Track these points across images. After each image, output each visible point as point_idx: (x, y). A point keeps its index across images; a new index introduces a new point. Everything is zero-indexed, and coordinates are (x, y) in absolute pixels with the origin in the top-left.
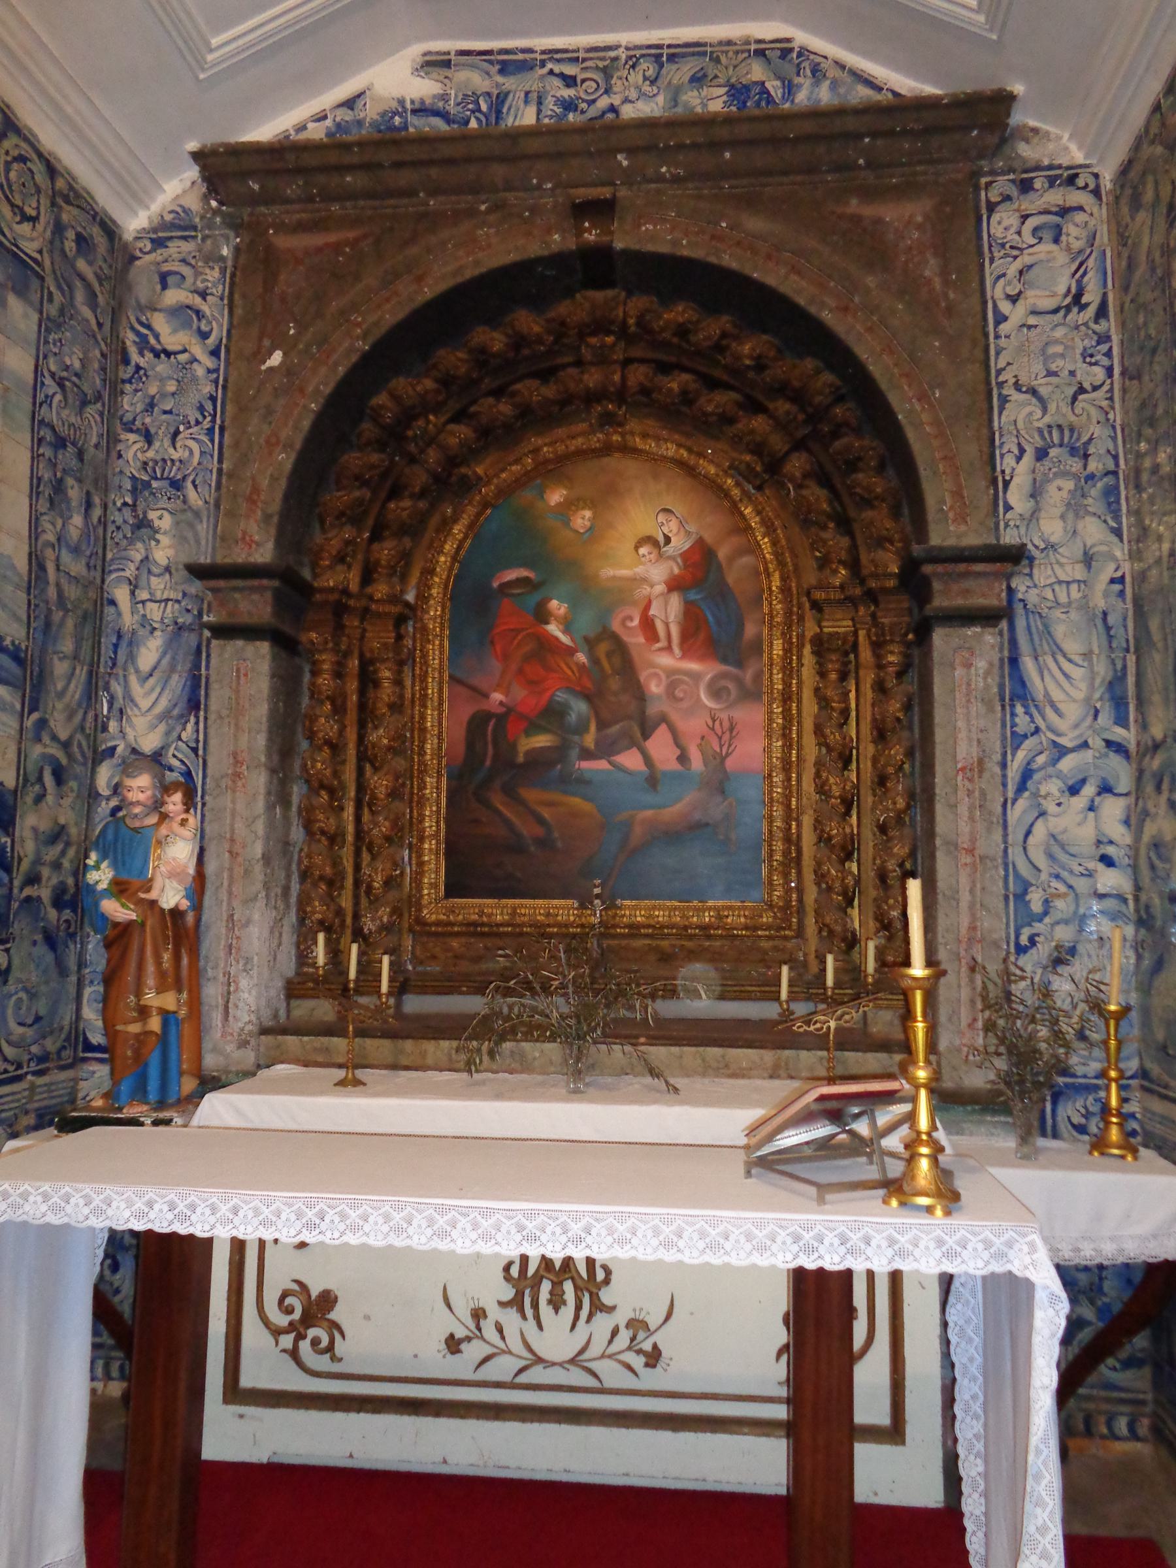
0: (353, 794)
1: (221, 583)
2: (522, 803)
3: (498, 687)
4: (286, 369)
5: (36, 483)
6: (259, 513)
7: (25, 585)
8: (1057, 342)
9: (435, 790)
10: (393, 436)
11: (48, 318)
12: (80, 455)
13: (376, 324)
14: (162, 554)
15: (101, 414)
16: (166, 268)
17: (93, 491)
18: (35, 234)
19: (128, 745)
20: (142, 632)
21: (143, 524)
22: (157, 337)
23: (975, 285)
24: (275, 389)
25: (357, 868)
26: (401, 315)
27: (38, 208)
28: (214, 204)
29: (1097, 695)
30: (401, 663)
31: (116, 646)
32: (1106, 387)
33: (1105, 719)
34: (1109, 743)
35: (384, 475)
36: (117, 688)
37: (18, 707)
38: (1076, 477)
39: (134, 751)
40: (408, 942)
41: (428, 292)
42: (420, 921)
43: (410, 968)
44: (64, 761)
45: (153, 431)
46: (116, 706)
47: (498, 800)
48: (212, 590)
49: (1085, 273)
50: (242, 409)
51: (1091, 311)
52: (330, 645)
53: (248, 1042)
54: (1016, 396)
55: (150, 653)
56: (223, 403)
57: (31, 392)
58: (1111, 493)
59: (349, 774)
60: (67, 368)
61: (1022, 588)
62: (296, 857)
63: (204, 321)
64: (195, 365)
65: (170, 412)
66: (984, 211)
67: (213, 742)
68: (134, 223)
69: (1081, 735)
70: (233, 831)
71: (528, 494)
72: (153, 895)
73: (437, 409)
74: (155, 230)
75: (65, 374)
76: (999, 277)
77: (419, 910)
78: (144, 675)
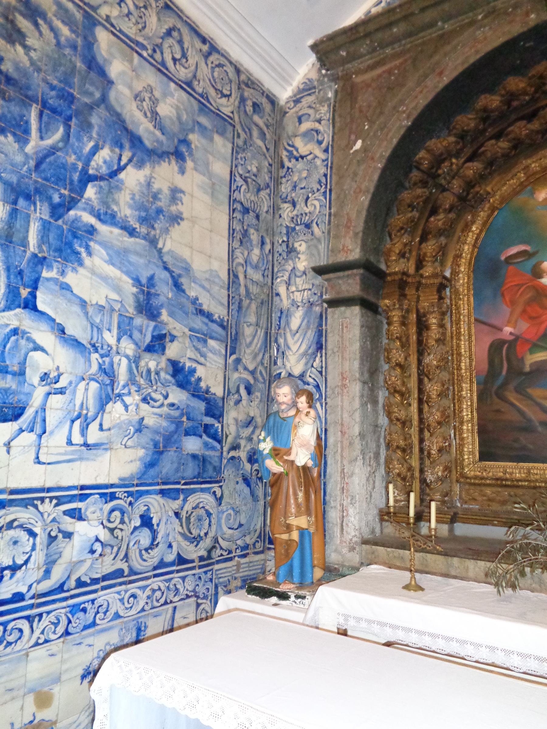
0: (416, 396)
1: (331, 275)
2: (529, 397)
3: (508, 323)
4: (365, 149)
5: (232, 232)
6: (351, 232)
7: (226, 286)
9: (469, 392)
10: (431, 176)
11: (237, 146)
12: (258, 217)
13: (415, 108)
14: (302, 264)
15: (269, 195)
16: (300, 113)
17: (265, 235)
18: (229, 103)
19: (287, 372)
20: (293, 309)
21: (291, 251)
22: (297, 150)
24: (358, 161)
25: (421, 441)
26: (431, 96)
27: (231, 90)
28: (324, 72)
30: (444, 314)
31: (280, 318)
35: (427, 201)
36: (281, 341)
37: (223, 352)
39: (290, 375)
40: (457, 488)
41: (446, 80)
42: (463, 475)
43: (459, 505)
44: (252, 381)
45: (296, 200)
46: (281, 350)
47: (512, 397)
48: (326, 280)
50: (341, 177)
52: (397, 306)
53: (355, 549)
55: (296, 320)
56: (331, 176)
57: (228, 186)
59: (413, 383)
60: (249, 172)
62: (383, 434)
63: (320, 135)
64: (316, 160)
65: (304, 188)
67: (330, 368)
68: (284, 95)
70: (342, 418)
71: (522, 197)
72: (291, 458)
73: (457, 155)
74: (295, 95)
75: (247, 175)
77: (463, 469)
78: (294, 332)
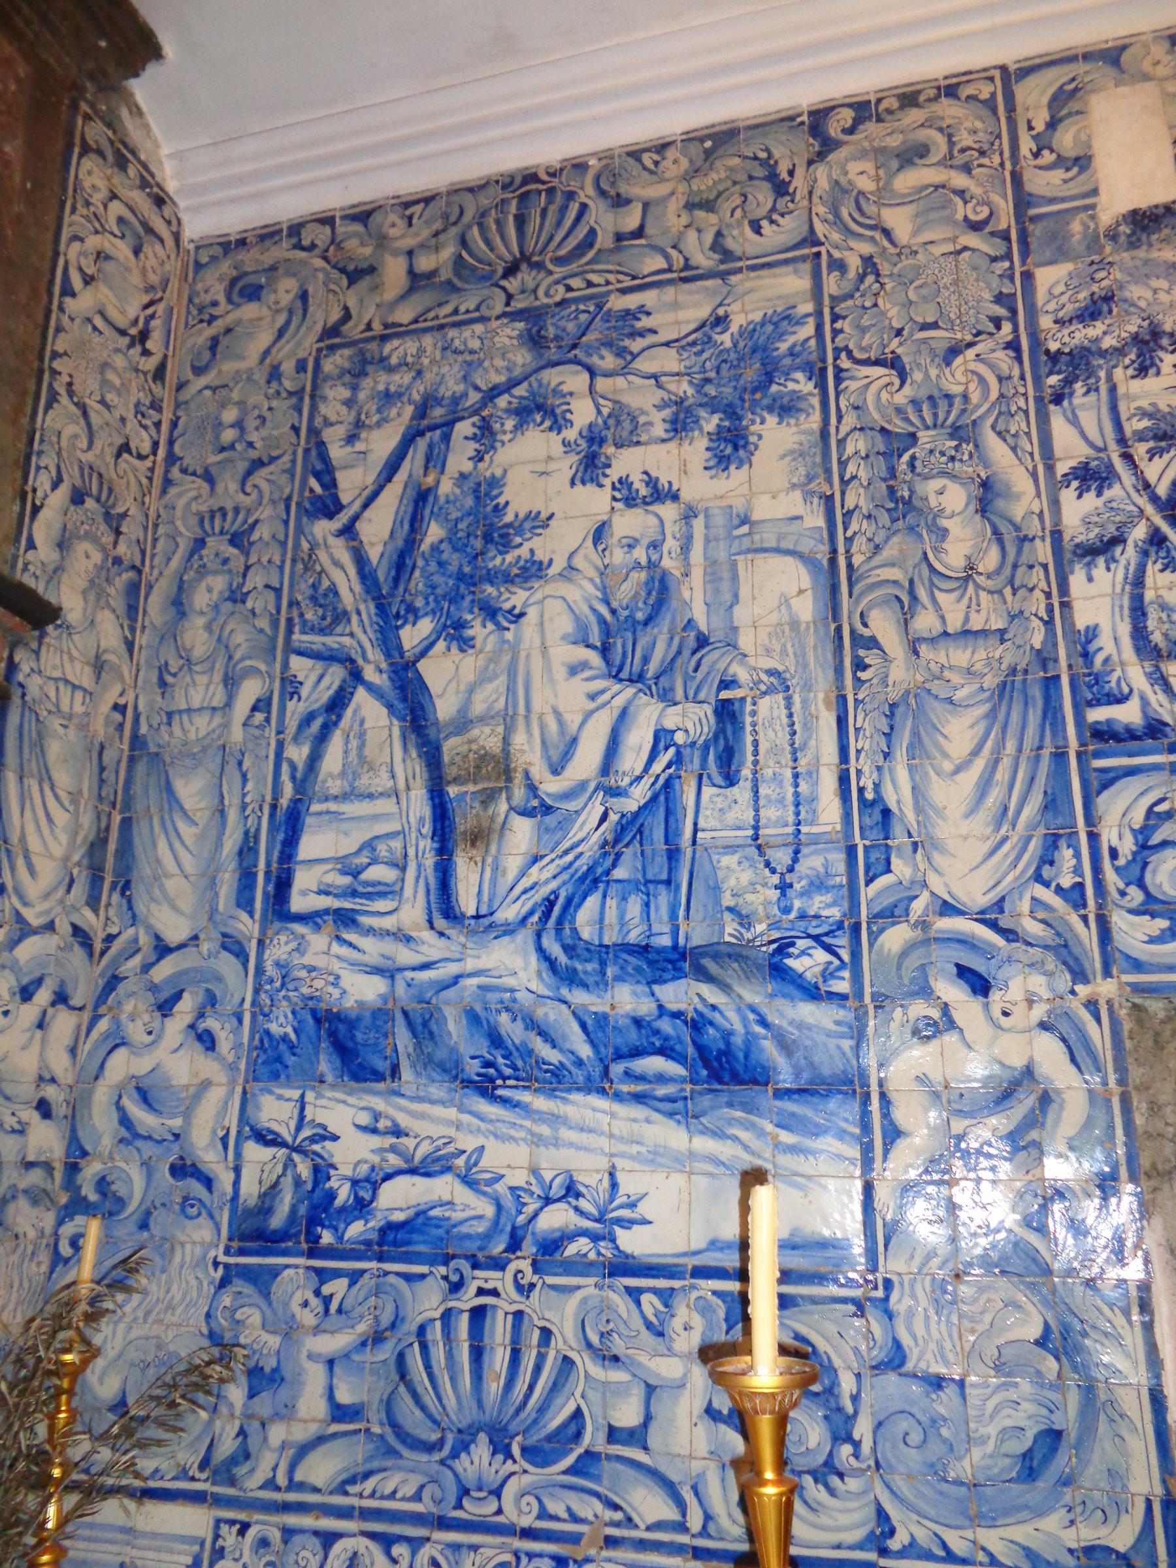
8: (115, 369)
23: (49, 219)
29: (76, 857)
32: (148, 463)
33: (80, 891)
34: (76, 930)
38: (103, 549)
49: (152, 317)
51: (150, 364)
54: (64, 400)
58: (133, 589)
61: (25, 668)
66: (77, 140)
69: (49, 911)
76: (76, 238)
